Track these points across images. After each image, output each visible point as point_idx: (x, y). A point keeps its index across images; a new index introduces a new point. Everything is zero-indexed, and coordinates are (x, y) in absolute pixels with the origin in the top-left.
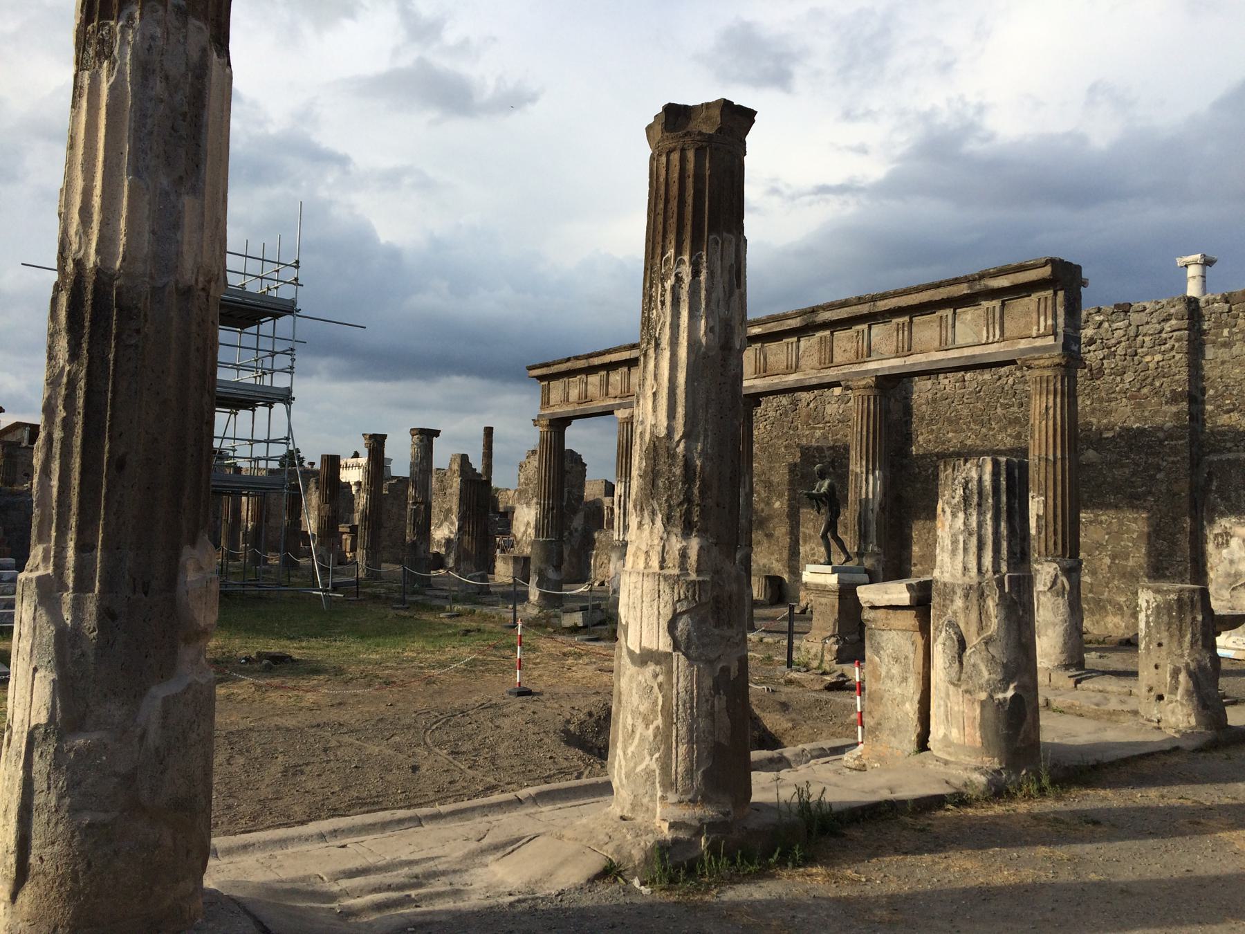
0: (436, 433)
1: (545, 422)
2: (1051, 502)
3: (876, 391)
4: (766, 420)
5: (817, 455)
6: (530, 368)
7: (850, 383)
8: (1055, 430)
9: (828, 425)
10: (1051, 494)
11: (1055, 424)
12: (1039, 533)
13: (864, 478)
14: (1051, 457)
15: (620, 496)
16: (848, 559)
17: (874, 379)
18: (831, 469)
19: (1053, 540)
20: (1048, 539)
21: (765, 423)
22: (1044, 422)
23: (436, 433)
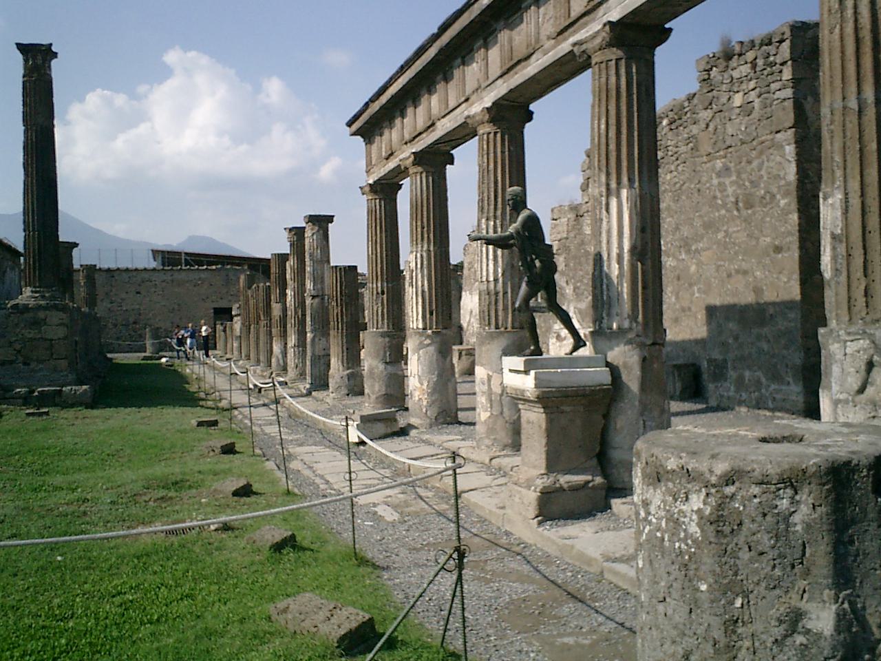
0: (330, 219)
1: (367, 189)
2: (855, 202)
3: (620, 53)
4: (677, 159)
5: (719, 195)
6: (350, 124)
7: (584, 47)
8: (858, 41)
9: (730, 150)
11: (857, 30)
12: (837, 271)
13: (604, 203)
14: (853, 104)
15: (413, 271)
16: (579, 343)
17: (607, 28)
18: (735, 213)
19: (863, 287)
20: (854, 284)
21: (676, 163)
22: (837, 30)
23: (330, 219)
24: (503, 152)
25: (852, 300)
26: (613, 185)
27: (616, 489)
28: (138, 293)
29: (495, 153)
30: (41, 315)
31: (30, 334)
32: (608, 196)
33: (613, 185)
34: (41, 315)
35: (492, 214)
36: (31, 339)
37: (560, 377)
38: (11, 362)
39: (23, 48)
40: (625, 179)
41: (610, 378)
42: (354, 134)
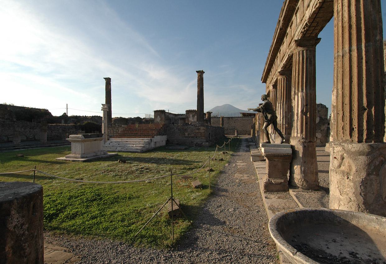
10: (340, 86)
24: (284, 84)
25: (339, 131)
26: (297, 92)
27: (293, 186)
28: (235, 122)
29: (281, 84)
30: (199, 127)
31: (197, 131)
32: (295, 95)
33: (297, 92)
34: (199, 127)
35: (280, 102)
36: (197, 132)
37: (273, 150)
38: (194, 137)
39: (197, 72)
40: (300, 89)
41: (291, 152)
42: (263, 83)
